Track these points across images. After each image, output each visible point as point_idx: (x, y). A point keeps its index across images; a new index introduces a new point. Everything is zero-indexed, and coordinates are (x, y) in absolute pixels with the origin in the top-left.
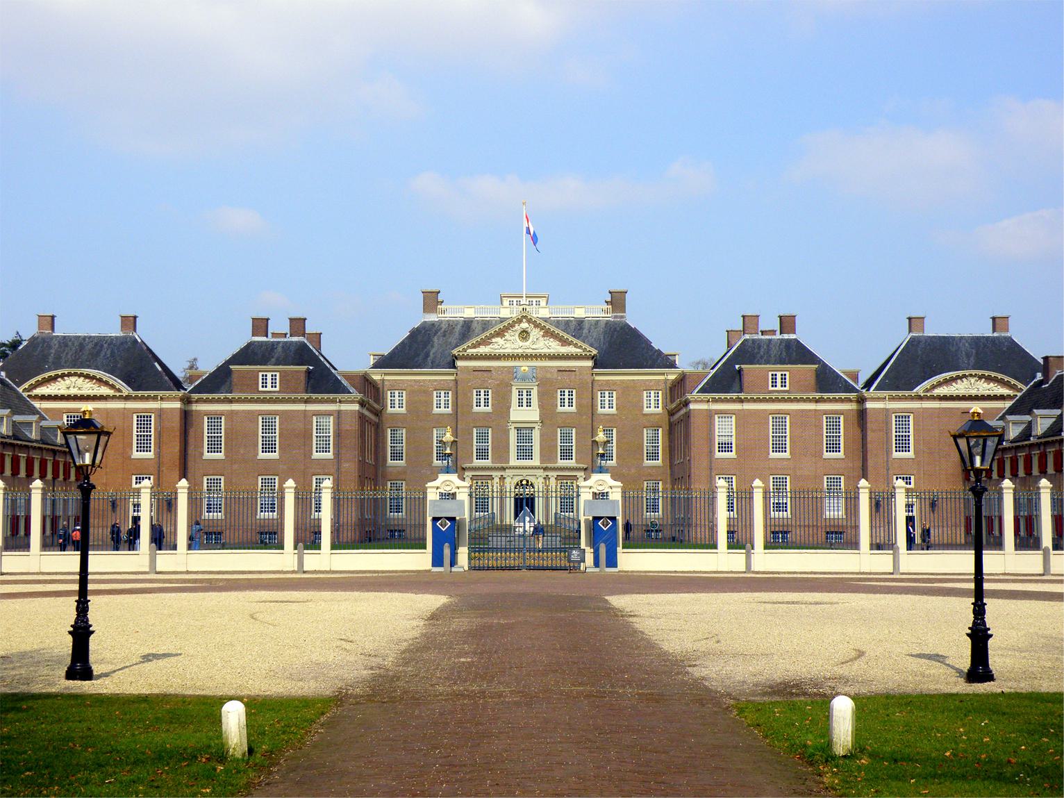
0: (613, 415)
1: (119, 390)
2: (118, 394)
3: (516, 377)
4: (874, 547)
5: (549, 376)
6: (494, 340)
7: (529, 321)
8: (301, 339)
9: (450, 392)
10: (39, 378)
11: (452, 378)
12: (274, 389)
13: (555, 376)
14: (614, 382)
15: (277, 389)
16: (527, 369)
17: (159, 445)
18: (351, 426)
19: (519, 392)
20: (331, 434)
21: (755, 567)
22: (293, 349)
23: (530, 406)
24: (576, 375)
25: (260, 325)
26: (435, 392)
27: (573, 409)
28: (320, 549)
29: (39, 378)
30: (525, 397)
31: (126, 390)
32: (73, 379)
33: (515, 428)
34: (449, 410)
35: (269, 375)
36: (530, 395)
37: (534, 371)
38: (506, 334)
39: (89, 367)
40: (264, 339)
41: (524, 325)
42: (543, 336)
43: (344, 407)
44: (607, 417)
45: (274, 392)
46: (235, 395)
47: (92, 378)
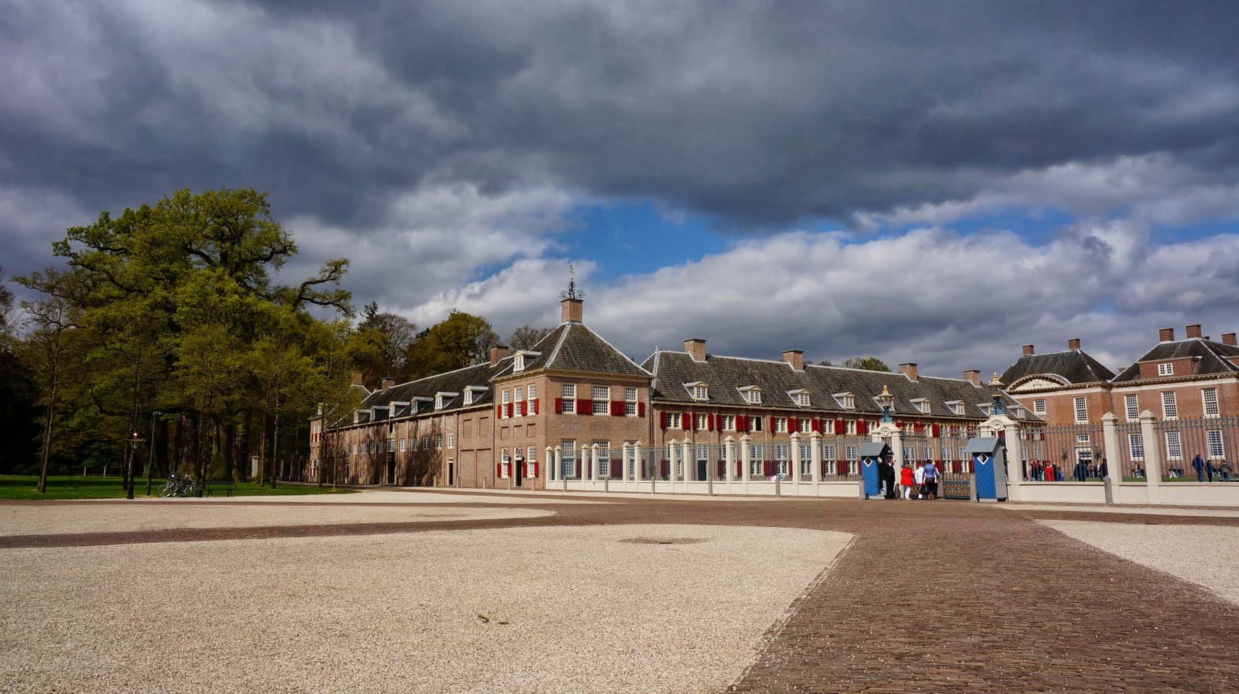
1: (1062, 384)
2: (1062, 387)
4: (833, 470)
8: (1199, 339)
10: (1017, 381)
12: (1169, 374)
15: (1172, 374)
17: (1090, 416)
18: (1231, 394)
20: (1217, 401)
21: (782, 493)
22: (1189, 346)
25: (1168, 333)
28: (811, 481)
29: (1017, 381)
31: (1068, 383)
32: (1036, 380)
35: (1165, 365)
39: (1048, 372)
40: (1170, 342)
43: (1224, 381)
45: (1170, 376)
46: (1142, 380)
47: (1046, 379)
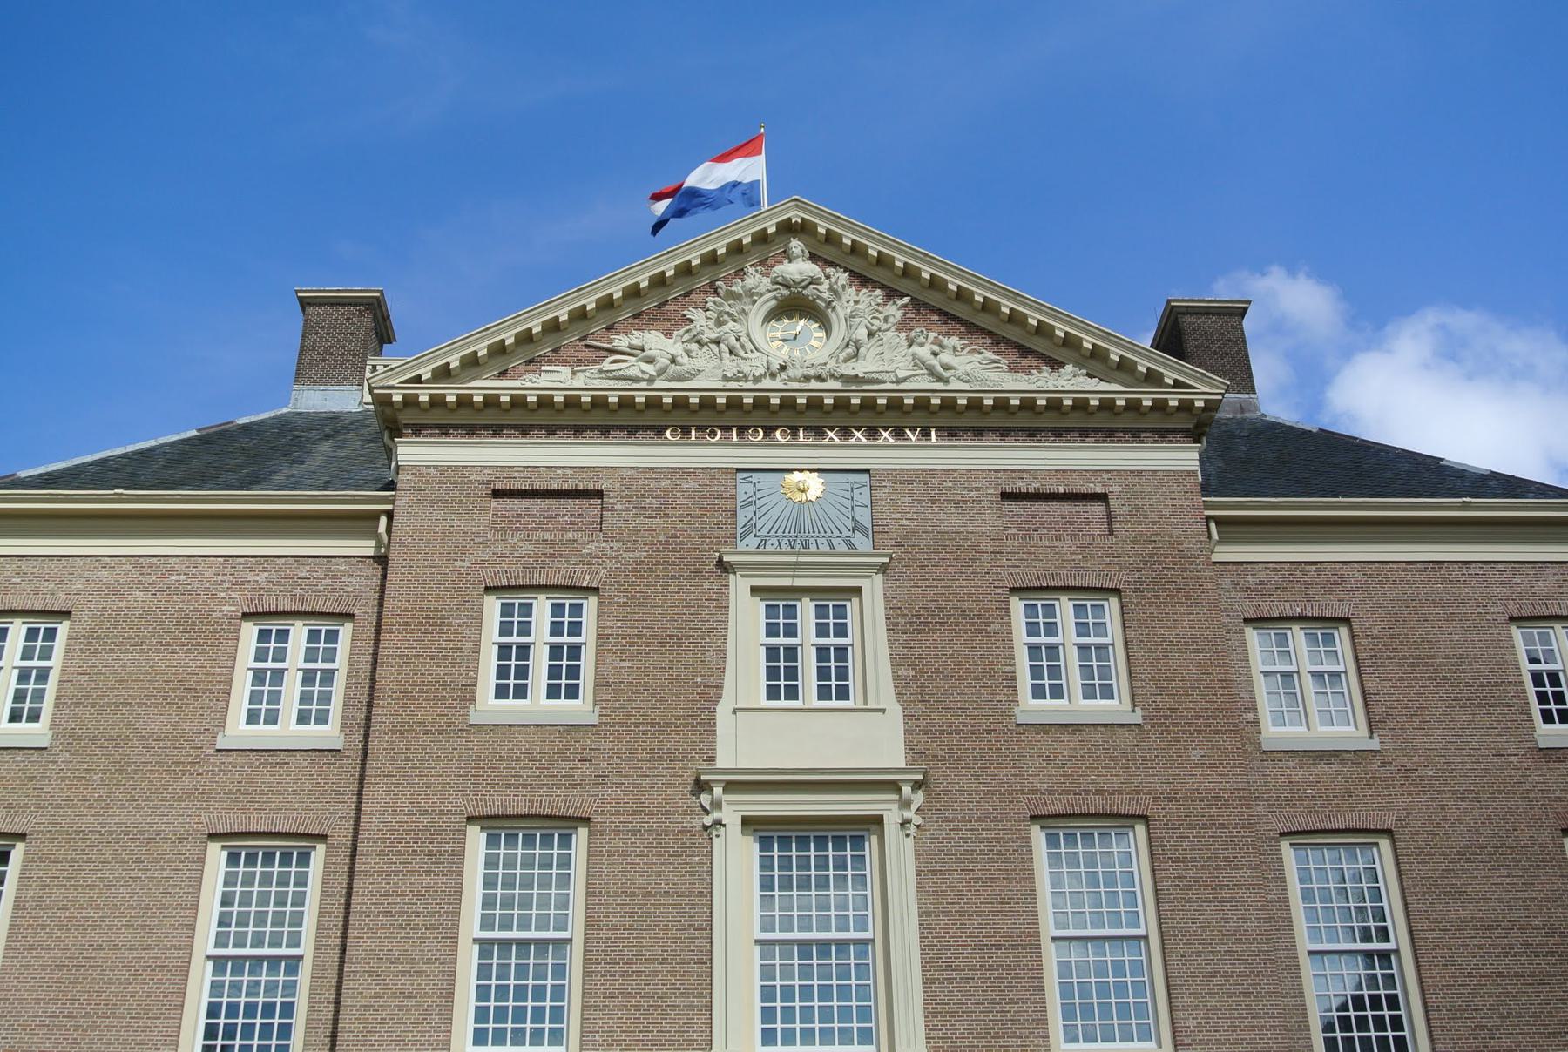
0: (1360, 756)
3: (750, 528)
5: (951, 520)
6: (621, 342)
7: (826, 250)
9: (346, 631)
11: (366, 547)
13: (989, 515)
14: (1335, 576)
16: (815, 485)
19: (771, 611)
23: (843, 693)
24: (1109, 515)
26: (250, 631)
27: (1117, 708)
30: (807, 636)
33: (748, 822)
34: (328, 734)
36: (841, 631)
37: (864, 496)
38: (691, 313)
41: (799, 268)
42: (903, 326)
44: (1328, 770)
